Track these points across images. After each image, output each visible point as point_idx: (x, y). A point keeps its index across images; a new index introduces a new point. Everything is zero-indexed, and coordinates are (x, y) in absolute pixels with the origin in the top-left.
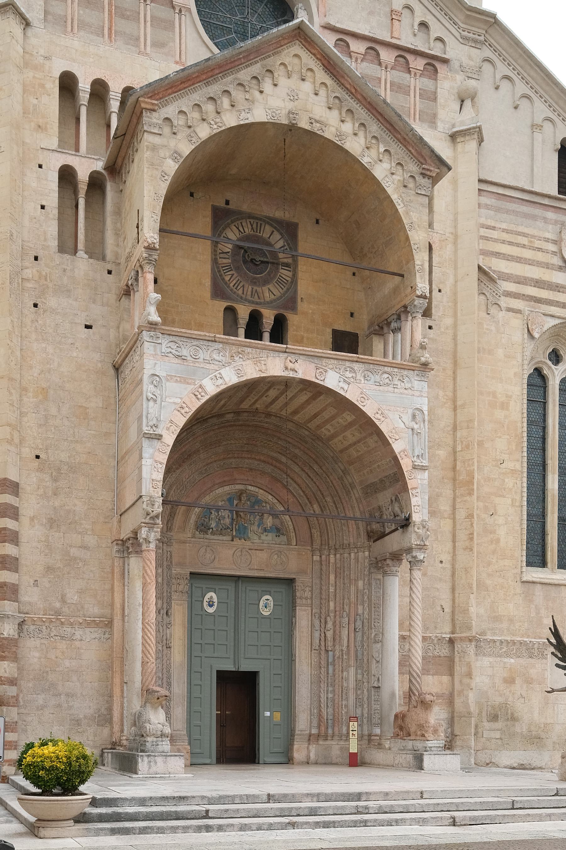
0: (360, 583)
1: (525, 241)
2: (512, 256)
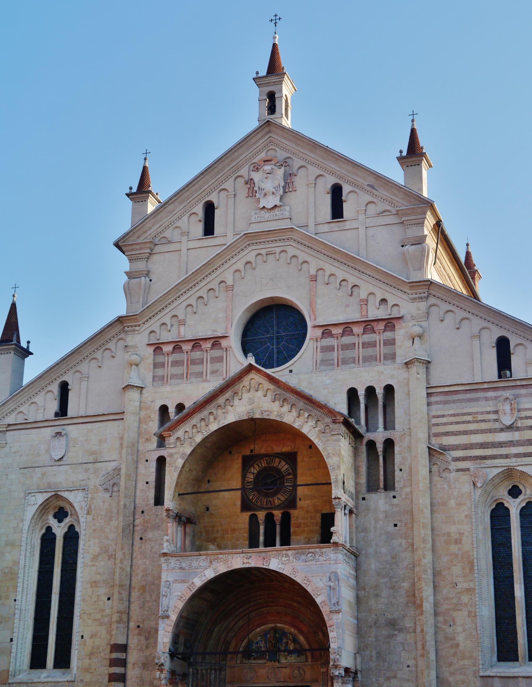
1: (469, 418)
2: (459, 431)
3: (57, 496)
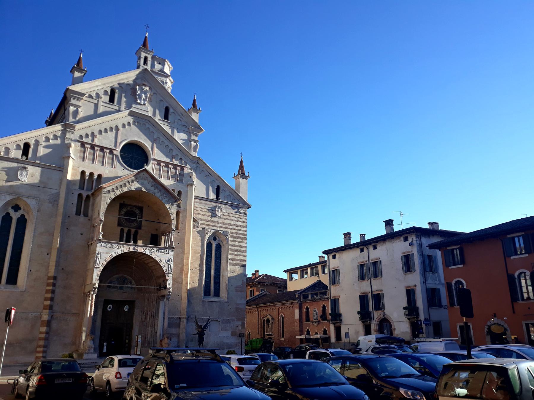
0: (154, 302)
3: (18, 198)
